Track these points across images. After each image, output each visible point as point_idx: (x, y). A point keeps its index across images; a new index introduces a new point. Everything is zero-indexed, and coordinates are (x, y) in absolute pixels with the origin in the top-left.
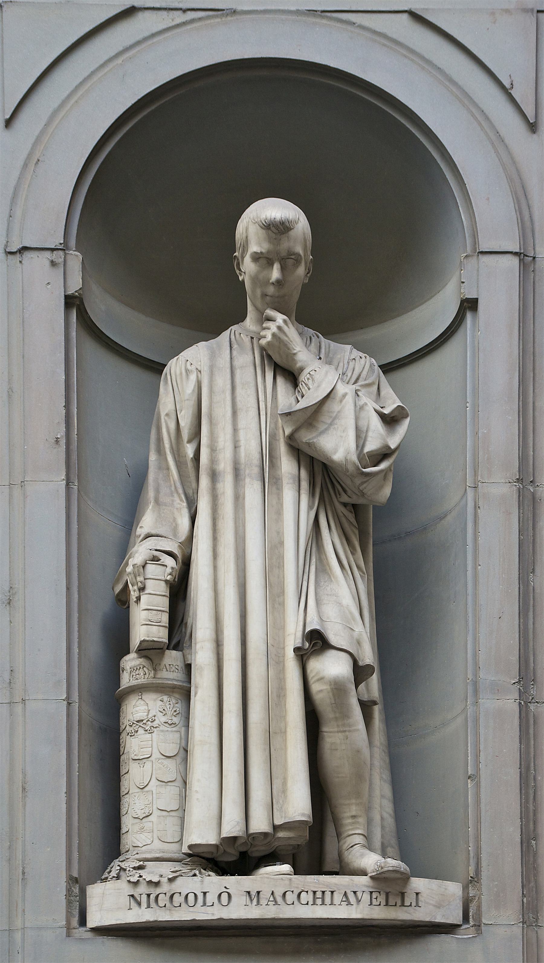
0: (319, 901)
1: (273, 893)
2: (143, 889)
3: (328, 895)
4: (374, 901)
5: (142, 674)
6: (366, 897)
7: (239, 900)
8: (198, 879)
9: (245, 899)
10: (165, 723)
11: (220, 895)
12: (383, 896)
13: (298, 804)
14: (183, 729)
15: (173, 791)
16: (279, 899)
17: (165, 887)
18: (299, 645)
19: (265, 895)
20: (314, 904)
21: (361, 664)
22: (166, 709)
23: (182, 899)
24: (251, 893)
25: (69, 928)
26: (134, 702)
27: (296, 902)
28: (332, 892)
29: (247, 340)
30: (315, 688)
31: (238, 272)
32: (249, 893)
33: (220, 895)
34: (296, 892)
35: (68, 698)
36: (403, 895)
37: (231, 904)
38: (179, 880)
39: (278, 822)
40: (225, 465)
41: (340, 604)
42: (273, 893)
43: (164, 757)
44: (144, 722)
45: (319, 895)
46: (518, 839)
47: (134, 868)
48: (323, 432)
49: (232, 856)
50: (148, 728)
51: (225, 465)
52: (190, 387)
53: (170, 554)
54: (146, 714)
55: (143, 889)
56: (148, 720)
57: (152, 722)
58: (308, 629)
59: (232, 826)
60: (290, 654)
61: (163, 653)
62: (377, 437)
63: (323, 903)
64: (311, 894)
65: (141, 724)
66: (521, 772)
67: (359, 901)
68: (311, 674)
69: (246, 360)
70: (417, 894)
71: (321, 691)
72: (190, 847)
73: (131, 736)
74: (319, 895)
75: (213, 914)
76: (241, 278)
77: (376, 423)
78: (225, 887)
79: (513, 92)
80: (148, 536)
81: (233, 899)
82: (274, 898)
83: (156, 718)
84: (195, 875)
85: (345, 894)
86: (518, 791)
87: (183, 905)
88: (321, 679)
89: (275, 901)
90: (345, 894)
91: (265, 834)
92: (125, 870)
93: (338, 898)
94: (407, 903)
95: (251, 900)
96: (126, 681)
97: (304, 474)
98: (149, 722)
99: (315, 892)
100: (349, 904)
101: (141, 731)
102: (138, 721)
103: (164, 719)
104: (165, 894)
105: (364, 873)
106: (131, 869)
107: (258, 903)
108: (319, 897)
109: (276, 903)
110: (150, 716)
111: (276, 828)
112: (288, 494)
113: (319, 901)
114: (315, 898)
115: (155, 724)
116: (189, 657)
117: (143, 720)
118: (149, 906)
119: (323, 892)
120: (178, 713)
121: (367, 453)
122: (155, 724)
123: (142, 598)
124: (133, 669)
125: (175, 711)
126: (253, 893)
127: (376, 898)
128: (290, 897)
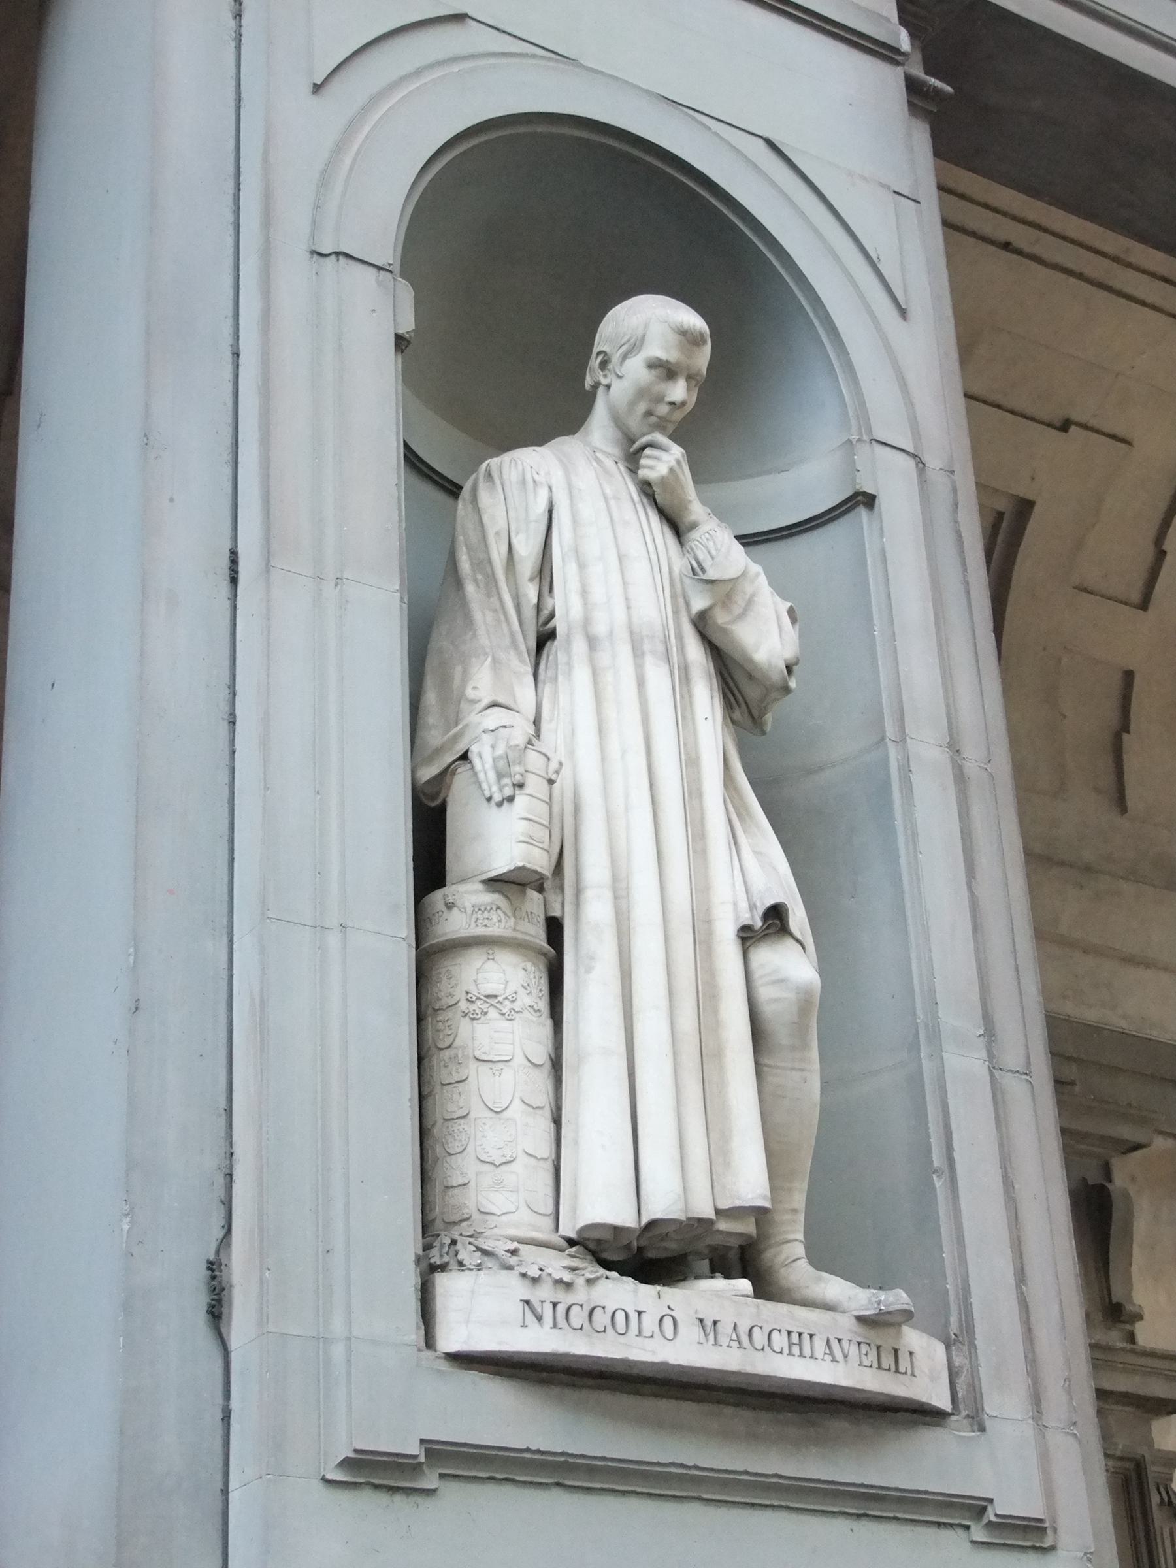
0: (796, 1350)
1: (735, 1328)
2: (544, 1293)
3: (806, 1338)
5: (495, 919)
6: (854, 1350)
7: (690, 1332)
11: (661, 1319)
12: (873, 1354)
15: (544, 1124)
17: (581, 1294)
19: (725, 1329)
20: (790, 1354)
26: (478, 964)
28: (811, 1336)
30: (765, 993)
32: (701, 1321)
33: (661, 1319)
39: (724, 1205)
44: (500, 999)
47: (508, 1251)
48: (742, 616)
52: (541, 507)
54: (502, 986)
55: (544, 1293)
59: (664, 1201)
61: (524, 893)
64: (785, 1335)
65: (493, 1001)
68: (757, 974)
71: (777, 1000)
73: (473, 1019)
75: (654, 1353)
79: (880, 266)
80: (494, 705)
85: (828, 1343)
89: (739, 1341)
90: (828, 1343)
98: (507, 1002)
99: (789, 1333)
100: (834, 1360)
101: (493, 1013)
102: (488, 996)
103: (528, 1001)
108: (797, 1341)
114: (790, 1344)
117: (496, 996)
118: (555, 1326)
119: (800, 1334)
122: (517, 1006)
123: (517, 799)
124: (478, 908)
126: (709, 1324)
128: (759, 1337)
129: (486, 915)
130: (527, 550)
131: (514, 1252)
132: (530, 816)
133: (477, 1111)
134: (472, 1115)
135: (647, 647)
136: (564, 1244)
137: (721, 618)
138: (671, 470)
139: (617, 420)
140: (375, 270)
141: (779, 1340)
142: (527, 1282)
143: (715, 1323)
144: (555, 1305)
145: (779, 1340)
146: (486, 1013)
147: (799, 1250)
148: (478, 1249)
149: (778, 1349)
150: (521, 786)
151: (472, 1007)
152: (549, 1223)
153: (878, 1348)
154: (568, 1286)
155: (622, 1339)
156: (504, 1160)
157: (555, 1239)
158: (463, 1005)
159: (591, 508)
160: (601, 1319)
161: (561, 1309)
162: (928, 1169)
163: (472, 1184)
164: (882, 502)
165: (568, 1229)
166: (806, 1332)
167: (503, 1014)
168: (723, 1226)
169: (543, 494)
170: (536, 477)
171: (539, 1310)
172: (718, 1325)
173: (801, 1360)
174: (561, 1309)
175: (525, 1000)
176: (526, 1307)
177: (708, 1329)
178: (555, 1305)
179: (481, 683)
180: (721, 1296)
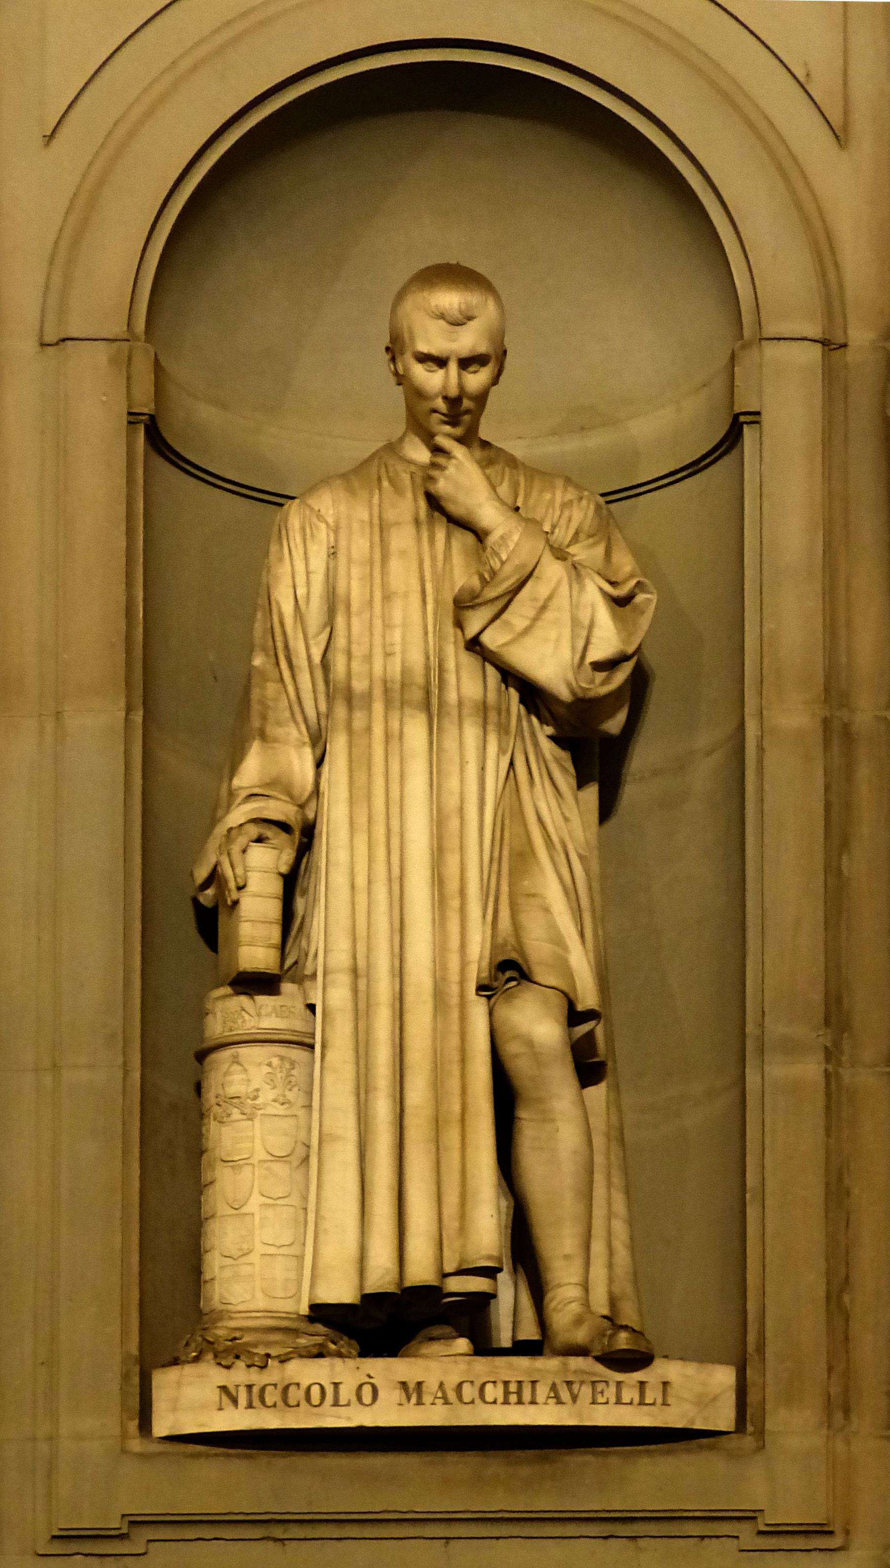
0: (513, 1398)
1: (441, 1385)
7: (390, 1396)
9: (397, 1395)
11: (360, 1387)
12: (613, 1389)
16: (452, 1396)
17: (274, 1374)
20: (506, 1402)
21: (580, 1008)
23: (301, 1394)
25: (124, 1435)
27: (478, 1401)
28: (534, 1383)
29: (406, 478)
32: (404, 1384)
33: (360, 1387)
34: (478, 1384)
35: (125, 1063)
37: (378, 1402)
42: (441, 1385)
45: (513, 1387)
46: (822, 1292)
50: (247, 1111)
53: (284, 827)
62: (607, 640)
63: (520, 1402)
64: (500, 1387)
66: (827, 1184)
67: (574, 1398)
74: (513, 1387)
77: (603, 615)
78: (369, 1376)
81: (381, 1394)
83: (260, 1093)
86: (823, 1214)
87: (303, 1403)
93: (542, 1391)
94: (648, 1400)
95: (409, 1399)
99: (506, 1383)
100: (559, 1402)
101: (236, 1114)
104: (275, 1385)
107: (419, 1403)
108: (514, 1393)
109: (447, 1402)
110: (251, 1089)
113: (513, 1398)
114: (507, 1393)
115: (259, 1101)
116: (312, 994)
118: (250, 1406)
121: (591, 663)
126: (412, 1386)
127: (602, 1392)
128: (469, 1392)
133: (222, 1209)
134: (219, 1214)
141: (491, 1392)
146: (229, 1115)
155: (316, 1410)
158: (216, 1109)
160: (295, 1395)
161: (255, 1390)
163: (217, 1278)
164: (765, 418)
172: (424, 1385)
173: (521, 1407)
177: (411, 1390)
178: (249, 1387)
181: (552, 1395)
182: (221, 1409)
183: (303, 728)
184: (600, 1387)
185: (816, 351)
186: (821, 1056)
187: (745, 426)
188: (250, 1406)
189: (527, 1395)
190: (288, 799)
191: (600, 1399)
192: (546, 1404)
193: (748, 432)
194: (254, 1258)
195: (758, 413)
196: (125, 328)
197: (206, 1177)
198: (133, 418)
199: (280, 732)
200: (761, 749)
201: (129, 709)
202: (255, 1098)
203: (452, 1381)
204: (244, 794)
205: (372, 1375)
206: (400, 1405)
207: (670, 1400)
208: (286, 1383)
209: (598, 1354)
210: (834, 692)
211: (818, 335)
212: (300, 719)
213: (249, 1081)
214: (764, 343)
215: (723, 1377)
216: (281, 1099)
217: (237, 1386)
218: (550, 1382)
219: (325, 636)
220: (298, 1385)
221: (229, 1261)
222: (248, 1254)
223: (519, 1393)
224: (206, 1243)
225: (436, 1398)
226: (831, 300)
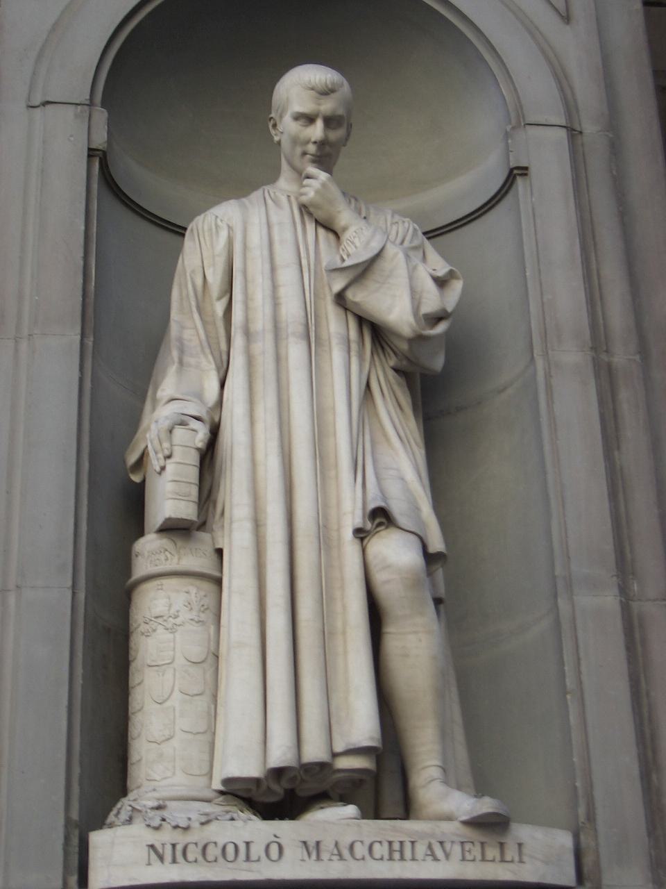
0: (397, 856)
1: (336, 844)
3: (408, 847)
4: (467, 854)
6: (457, 849)
7: (293, 851)
8: (239, 823)
9: (301, 852)
10: (192, 620)
13: (361, 725)
14: (212, 629)
15: (202, 703)
16: (346, 853)
18: (360, 525)
19: (328, 845)
20: (391, 859)
22: (191, 603)
23: (218, 852)
24: (308, 843)
29: (284, 199)
30: (379, 577)
31: (273, 132)
32: (305, 843)
34: (367, 843)
36: (502, 845)
38: (213, 827)
39: (339, 747)
40: (262, 321)
41: (402, 479)
42: (336, 844)
43: (189, 663)
44: (165, 618)
45: (396, 846)
47: (152, 808)
49: (279, 789)
50: (169, 626)
51: (262, 321)
54: (167, 608)
55: (166, 837)
56: (170, 616)
57: (175, 618)
58: (371, 506)
59: (280, 755)
60: (348, 534)
62: (432, 300)
63: (402, 858)
64: (386, 845)
65: (160, 620)
67: (447, 856)
69: (284, 217)
70: (520, 845)
71: (387, 582)
72: (227, 781)
74: (396, 846)
76: (276, 139)
77: (430, 285)
78: (275, 836)
81: (287, 852)
82: (338, 850)
83: (180, 614)
84: (232, 819)
85: (430, 847)
87: (221, 859)
88: (387, 567)
90: (430, 847)
91: (322, 766)
92: (139, 811)
93: (421, 849)
94: (508, 858)
96: (142, 567)
97: (353, 333)
98: (171, 619)
99: (390, 843)
100: (436, 859)
101: (160, 630)
102: (156, 617)
103: (189, 616)
104: (196, 844)
105: (449, 818)
106: (149, 811)
107: (318, 858)
108: (396, 851)
110: (173, 611)
111: (335, 755)
112: (337, 356)
113: (397, 856)
114: (391, 851)
115: (178, 621)
116: (220, 540)
117: (161, 616)
118: (174, 861)
120: (207, 609)
122: (178, 621)
125: (203, 605)
126: (312, 844)
128: (360, 850)
129: (157, 556)
130: (215, 279)
131: (159, 808)
132: (176, 479)
135: (290, 330)
136: (215, 794)
137: (354, 296)
138: (317, 192)
139: (290, 164)
140: (74, 106)
141: (379, 850)
142: (150, 830)
143: (318, 843)
144: (174, 846)
145: (379, 850)
146: (154, 631)
147: (435, 772)
148: (134, 809)
149: (377, 856)
150: (169, 457)
151: (147, 627)
152: (203, 781)
153: (482, 844)
154: (186, 829)
155: (230, 865)
156: (164, 738)
157: (208, 794)
159: (256, 237)
160: (213, 852)
161: (179, 848)
162: (564, 691)
164: (533, 171)
165: (217, 785)
166: (407, 840)
167: (167, 629)
168: (345, 763)
169: (224, 234)
170: (219, 223)
171: (161, 851)
174: (179, 848)
175: (185, 615)
176: (151, 850)
177: (311, 849)
178: (174, 846)
179: (168, 386)
180: (335, 820)
181: (429, 853)
182: (149, 864)
183: (210, 357)
184: (467, 847)
185: (563, 133)
186: (616, 591)
187: (518, 177)
188: (174, 861)
189: (408, 854)
190: (199, 402)
191: (468, 857)
192: (424, 860)
193: (519, 181)
194: (175, 743)
195: (526, 168)
196: (88, 97)
197: (134, 679)
198: (92, 153)
199: (192, 361)
200: (548, 376)
201: (83, 335)
202: (176, 617)
203: (345, 841)
204: (165, 400)
205: (278, 836)
206: (303, 860)
207: (525, 858)
208: (205, 842)
209: (464, 818)
210: (599, 341)
211: (564, 124)
212: (208, 351)
213: (170, 606)
214: (527, 127)
215: (564, 840)
216: (196, 619)
217: (163, 845)
218: (426, 842)
219: (225, 300)
220: (215, 843)
221: (154, 745)
222: (168, 739)
223: (402, 852)
224: (134, 730)
225: (333, 854)
226: (570, 106)
